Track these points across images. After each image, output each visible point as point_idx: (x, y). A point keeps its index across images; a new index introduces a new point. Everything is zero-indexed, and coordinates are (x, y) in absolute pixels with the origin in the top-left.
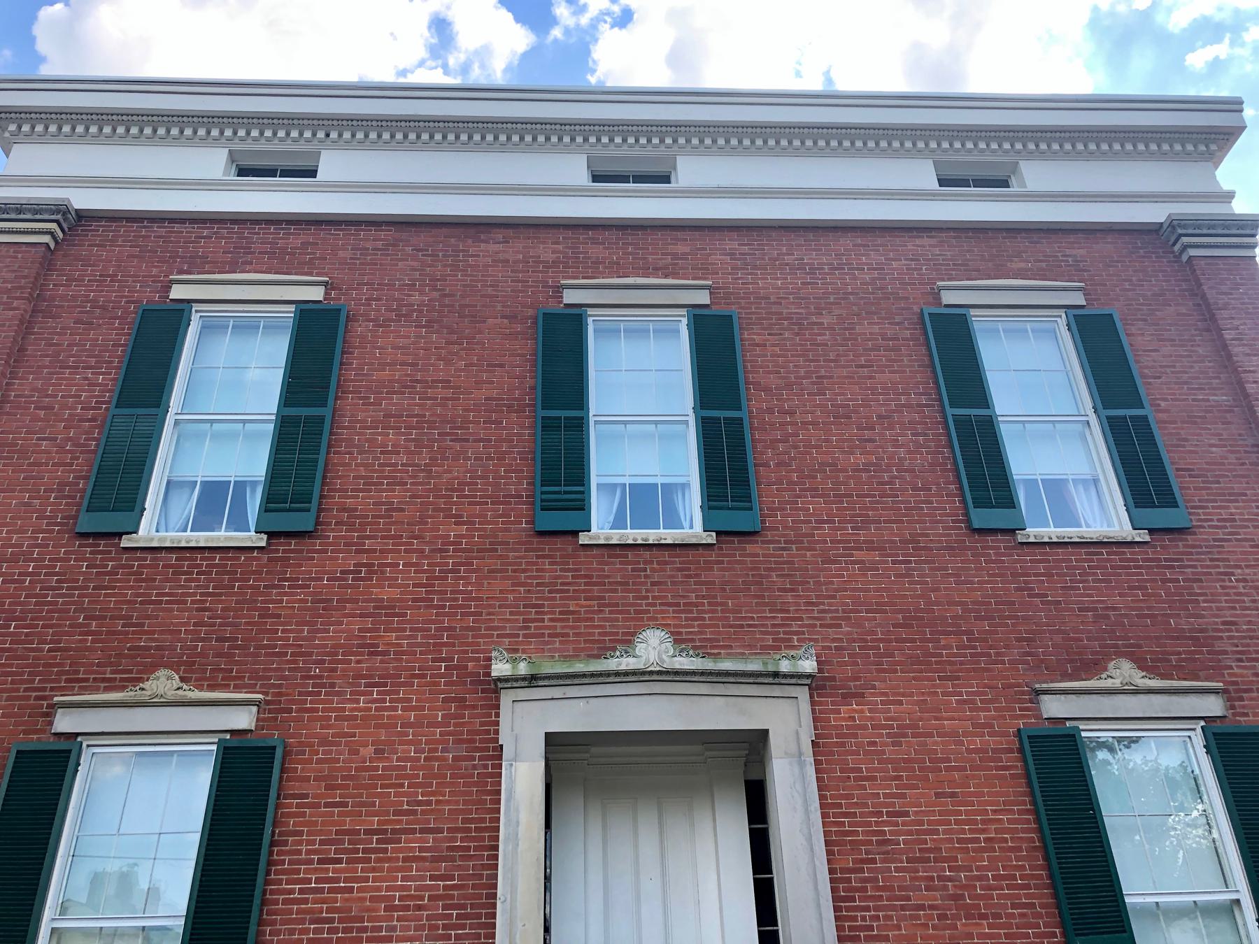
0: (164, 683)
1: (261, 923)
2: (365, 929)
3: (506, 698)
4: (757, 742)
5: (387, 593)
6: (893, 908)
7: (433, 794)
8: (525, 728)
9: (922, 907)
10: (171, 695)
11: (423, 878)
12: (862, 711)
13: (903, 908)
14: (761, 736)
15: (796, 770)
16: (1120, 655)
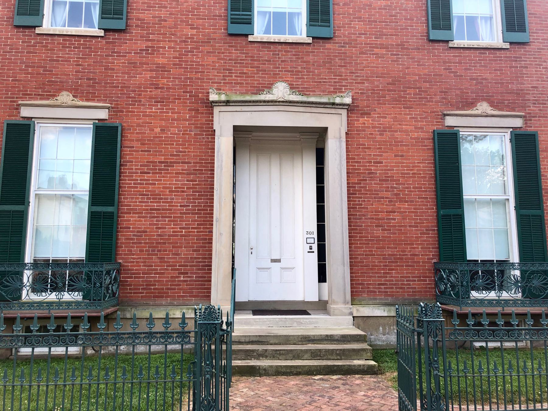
0: (65, 97)
1: (119, 195)
2: (162, 199)
3: (216, 110)
4: (322, 132)
5: (161, 61)
6: (371, 198)
7: (186, 148)
8: (225, 123)
9: (383, 198)
10: (70, 103)
11: (184, 181)
12: (369, 121)
13: (375, 198)
14: (325, 129)
15: (338, 143)
16: (483, 100)
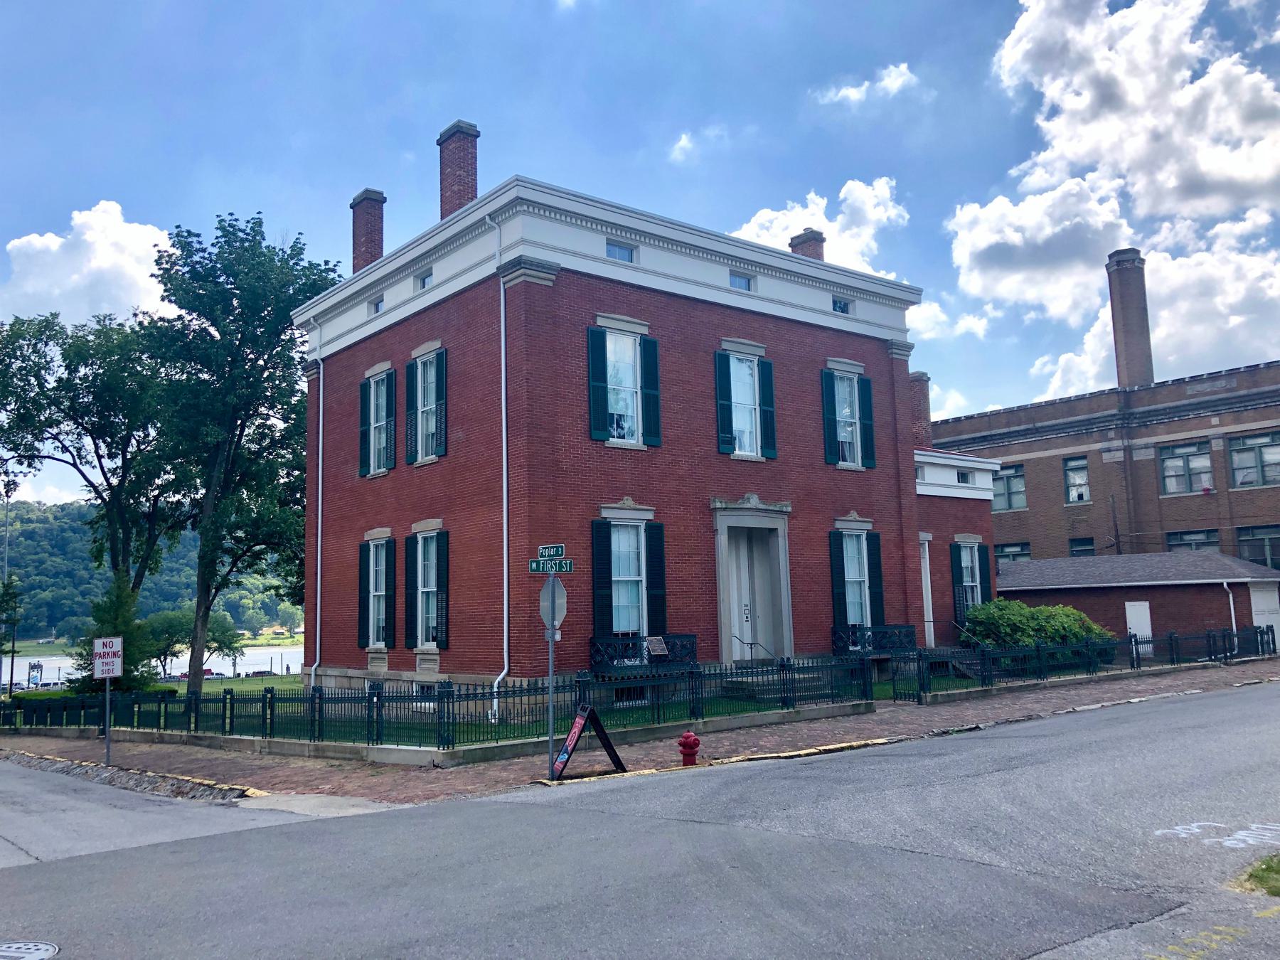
8: (723, 523)
